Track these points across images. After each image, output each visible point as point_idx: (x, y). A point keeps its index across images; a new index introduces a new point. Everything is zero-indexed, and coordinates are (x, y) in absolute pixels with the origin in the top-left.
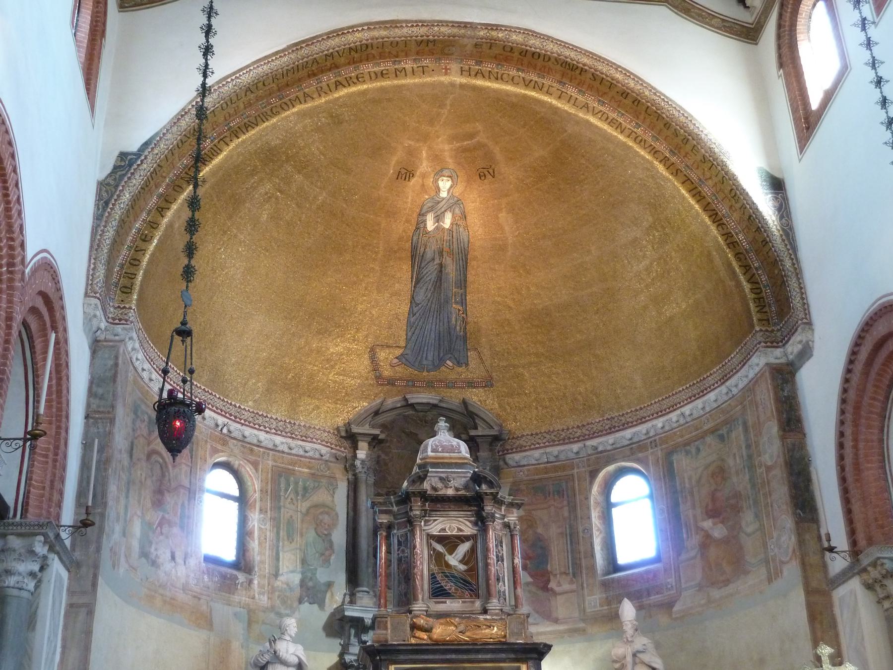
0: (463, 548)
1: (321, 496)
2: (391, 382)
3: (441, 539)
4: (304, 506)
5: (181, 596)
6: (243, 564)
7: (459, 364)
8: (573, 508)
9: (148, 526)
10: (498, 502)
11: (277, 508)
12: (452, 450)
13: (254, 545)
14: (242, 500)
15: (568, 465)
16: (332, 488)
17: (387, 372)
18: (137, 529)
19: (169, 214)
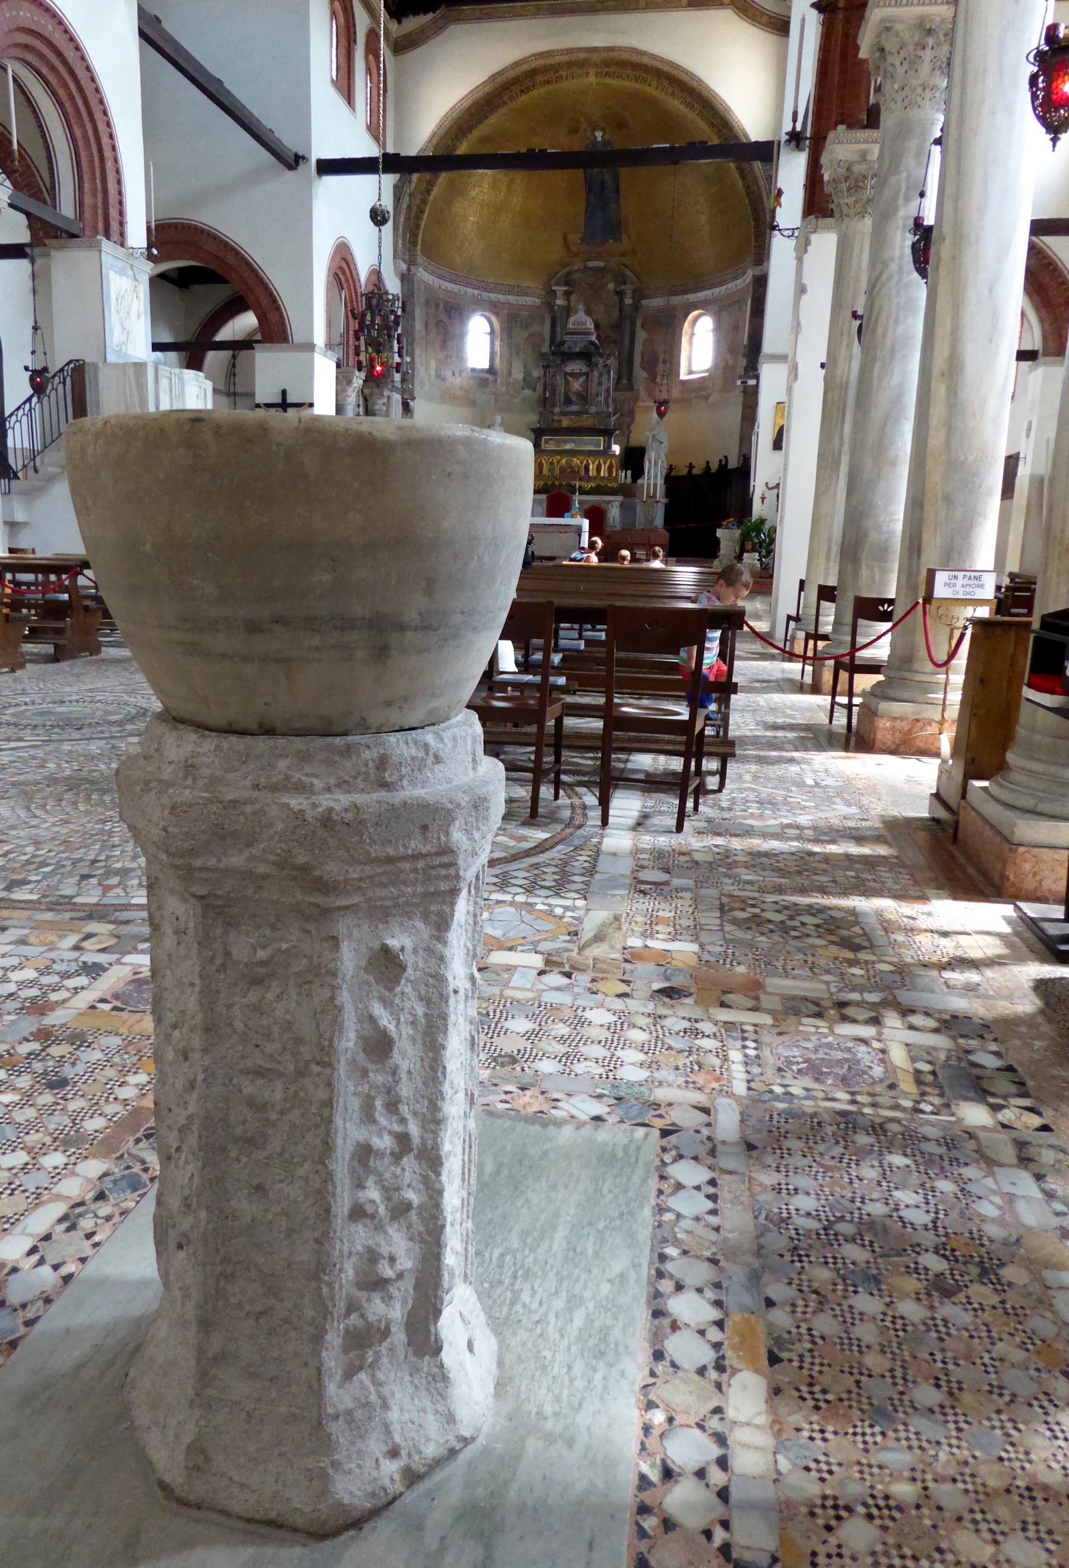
0: (582, 379)
1: (536, 328)
2: (576, 254)
3: (573, 375)
4: (525, 334)
5: (459, 393)
6: (491, 370)
7: (615, 240)
8: (673, 336)
9: (439, 361)
10: (601, 355)
11: (510, 337)
12: (582, 324)
13: (498, 360)
14: (492, 333)
15: (674, 308)
16: (542, 322)
17: (574, 249)
18: (433, 365)
19: (433, 194)
